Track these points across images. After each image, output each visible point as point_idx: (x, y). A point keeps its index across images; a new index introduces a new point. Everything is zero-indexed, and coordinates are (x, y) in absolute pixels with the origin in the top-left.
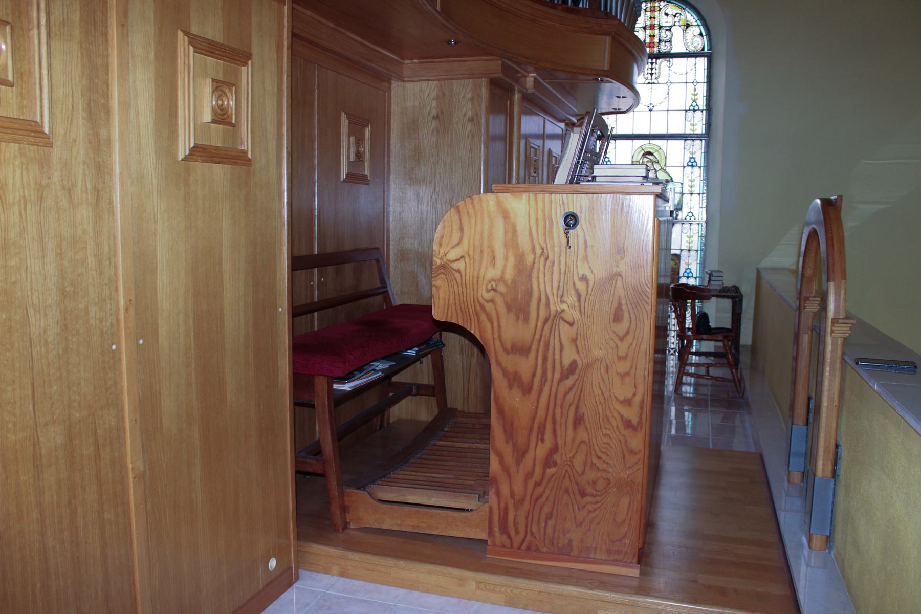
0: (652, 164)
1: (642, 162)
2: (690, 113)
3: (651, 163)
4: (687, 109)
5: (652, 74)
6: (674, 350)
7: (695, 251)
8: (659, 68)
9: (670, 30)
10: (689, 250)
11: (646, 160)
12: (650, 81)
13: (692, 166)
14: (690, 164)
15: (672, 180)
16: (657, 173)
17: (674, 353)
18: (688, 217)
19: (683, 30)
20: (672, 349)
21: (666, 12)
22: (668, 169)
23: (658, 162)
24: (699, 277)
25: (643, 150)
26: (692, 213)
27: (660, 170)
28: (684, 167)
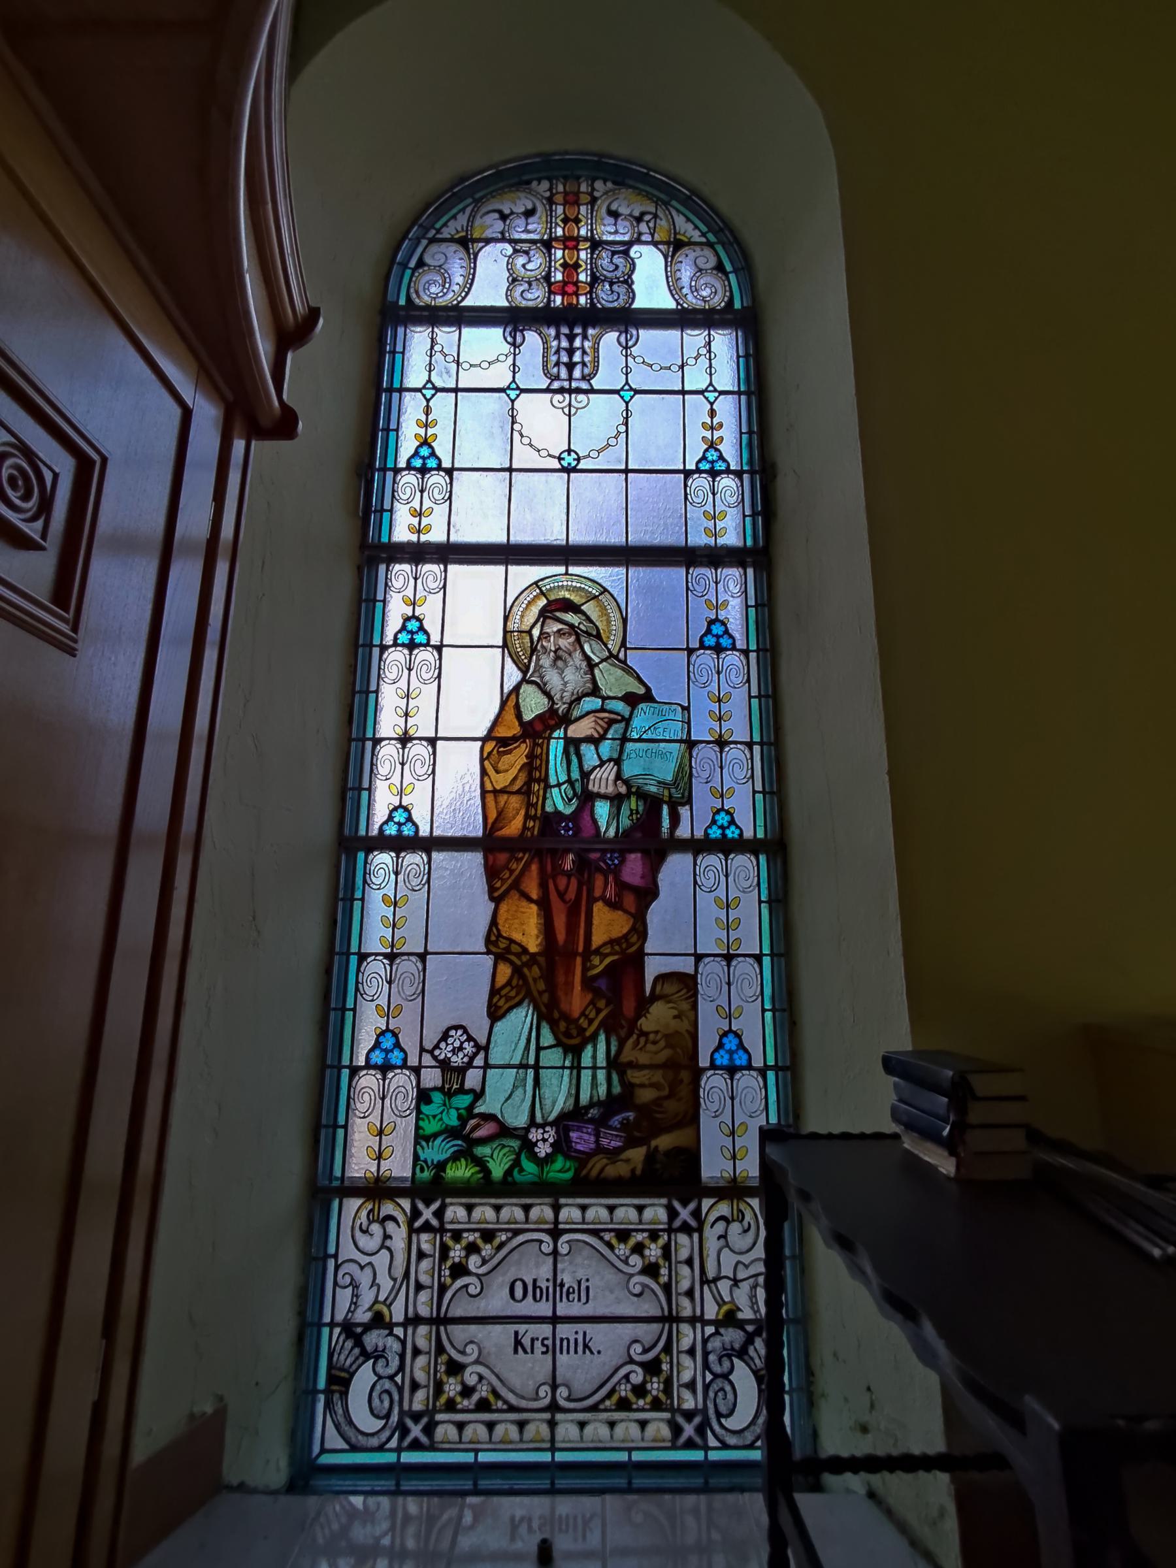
0: (578, 640)
1: (541, 633)
2: (700, 482)
3: (572, 639)
4: (691, 466)
5: (571, 366)
6: (697, 1420)
7: (751, 960)
8: (596, 350)
9: (626, 253)
10: (729, 958)
11: (553, 627)
12: (566, 384)
13: (718, 649)
14: (710, 641)
15: (648, 697)
16: (596, 671)
17: (698, 1440)
18: (715, 828)
19: (666, 257)
20: (689, 1415)
21: (614, 207)
22: (633, 659)
23: (598, 636)
24: (776, 1068)
25: (542, 593)
26: (728, 812)
27: (602, 661)
28: (690, 651)
